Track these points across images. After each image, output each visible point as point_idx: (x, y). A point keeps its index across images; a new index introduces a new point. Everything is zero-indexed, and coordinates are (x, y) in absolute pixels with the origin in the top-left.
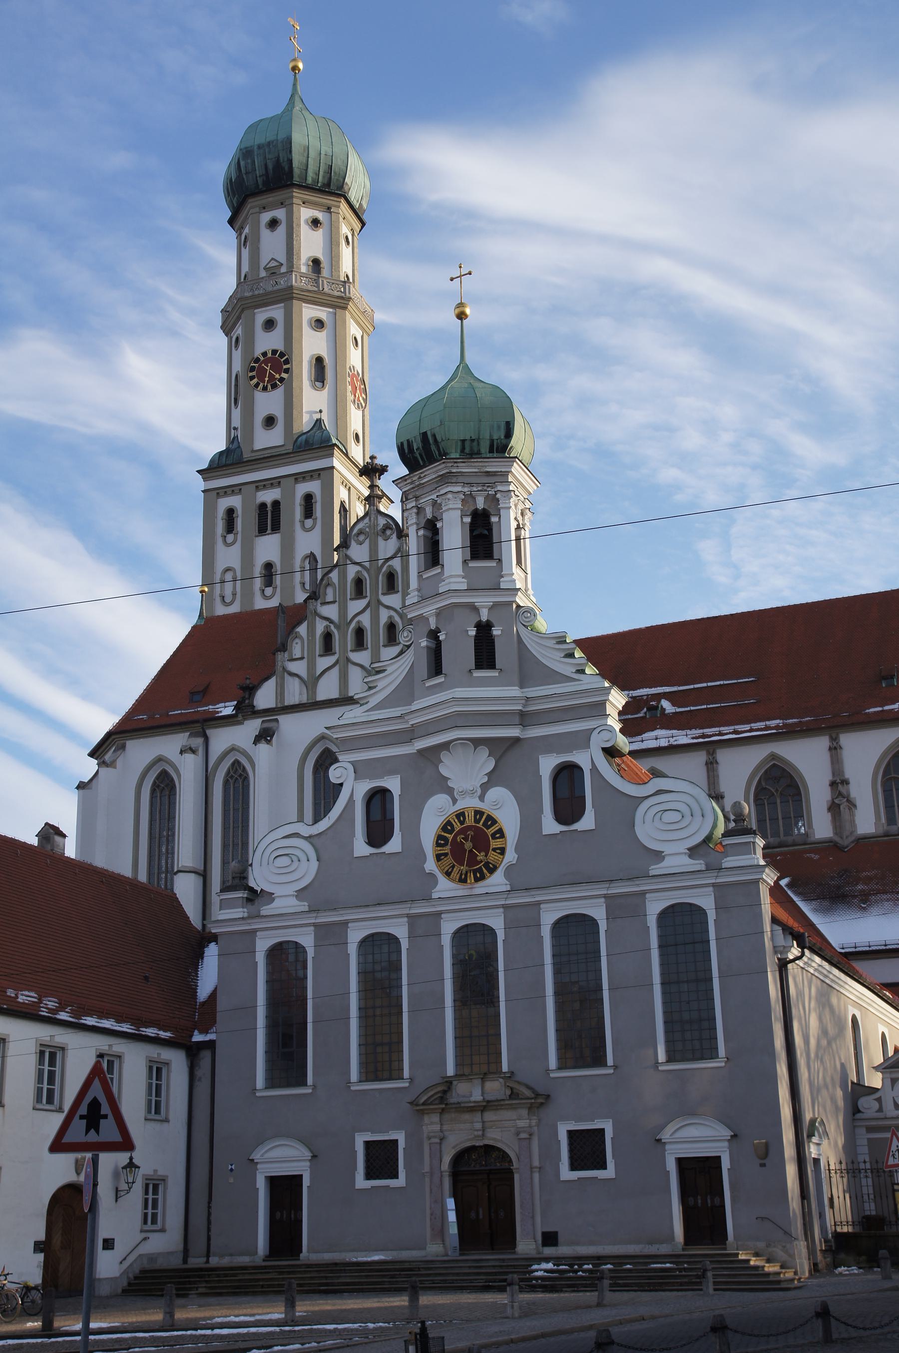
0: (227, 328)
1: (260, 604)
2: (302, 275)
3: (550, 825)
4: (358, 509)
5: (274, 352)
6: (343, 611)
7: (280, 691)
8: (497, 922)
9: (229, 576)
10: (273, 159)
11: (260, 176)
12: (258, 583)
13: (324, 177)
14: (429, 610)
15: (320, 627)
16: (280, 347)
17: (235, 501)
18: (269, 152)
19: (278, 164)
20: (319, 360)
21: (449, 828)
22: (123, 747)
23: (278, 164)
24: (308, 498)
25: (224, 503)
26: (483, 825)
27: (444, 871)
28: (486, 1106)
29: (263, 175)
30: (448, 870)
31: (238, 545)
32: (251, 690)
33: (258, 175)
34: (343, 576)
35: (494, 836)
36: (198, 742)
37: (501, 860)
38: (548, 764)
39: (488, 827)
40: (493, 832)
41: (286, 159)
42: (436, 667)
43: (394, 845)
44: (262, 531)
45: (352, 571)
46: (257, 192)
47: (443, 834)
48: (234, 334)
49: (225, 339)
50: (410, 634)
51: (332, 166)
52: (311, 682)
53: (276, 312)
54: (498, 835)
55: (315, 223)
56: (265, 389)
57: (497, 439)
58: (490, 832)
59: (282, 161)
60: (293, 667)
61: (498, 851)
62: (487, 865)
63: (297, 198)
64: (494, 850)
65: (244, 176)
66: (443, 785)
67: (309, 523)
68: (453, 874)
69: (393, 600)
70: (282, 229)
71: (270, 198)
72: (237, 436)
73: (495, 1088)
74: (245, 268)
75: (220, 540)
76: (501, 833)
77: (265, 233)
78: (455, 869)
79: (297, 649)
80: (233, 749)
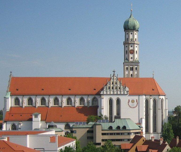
5: (132, 50)
20: (136, 51)
25: (126, 67)
53: (132, 45)
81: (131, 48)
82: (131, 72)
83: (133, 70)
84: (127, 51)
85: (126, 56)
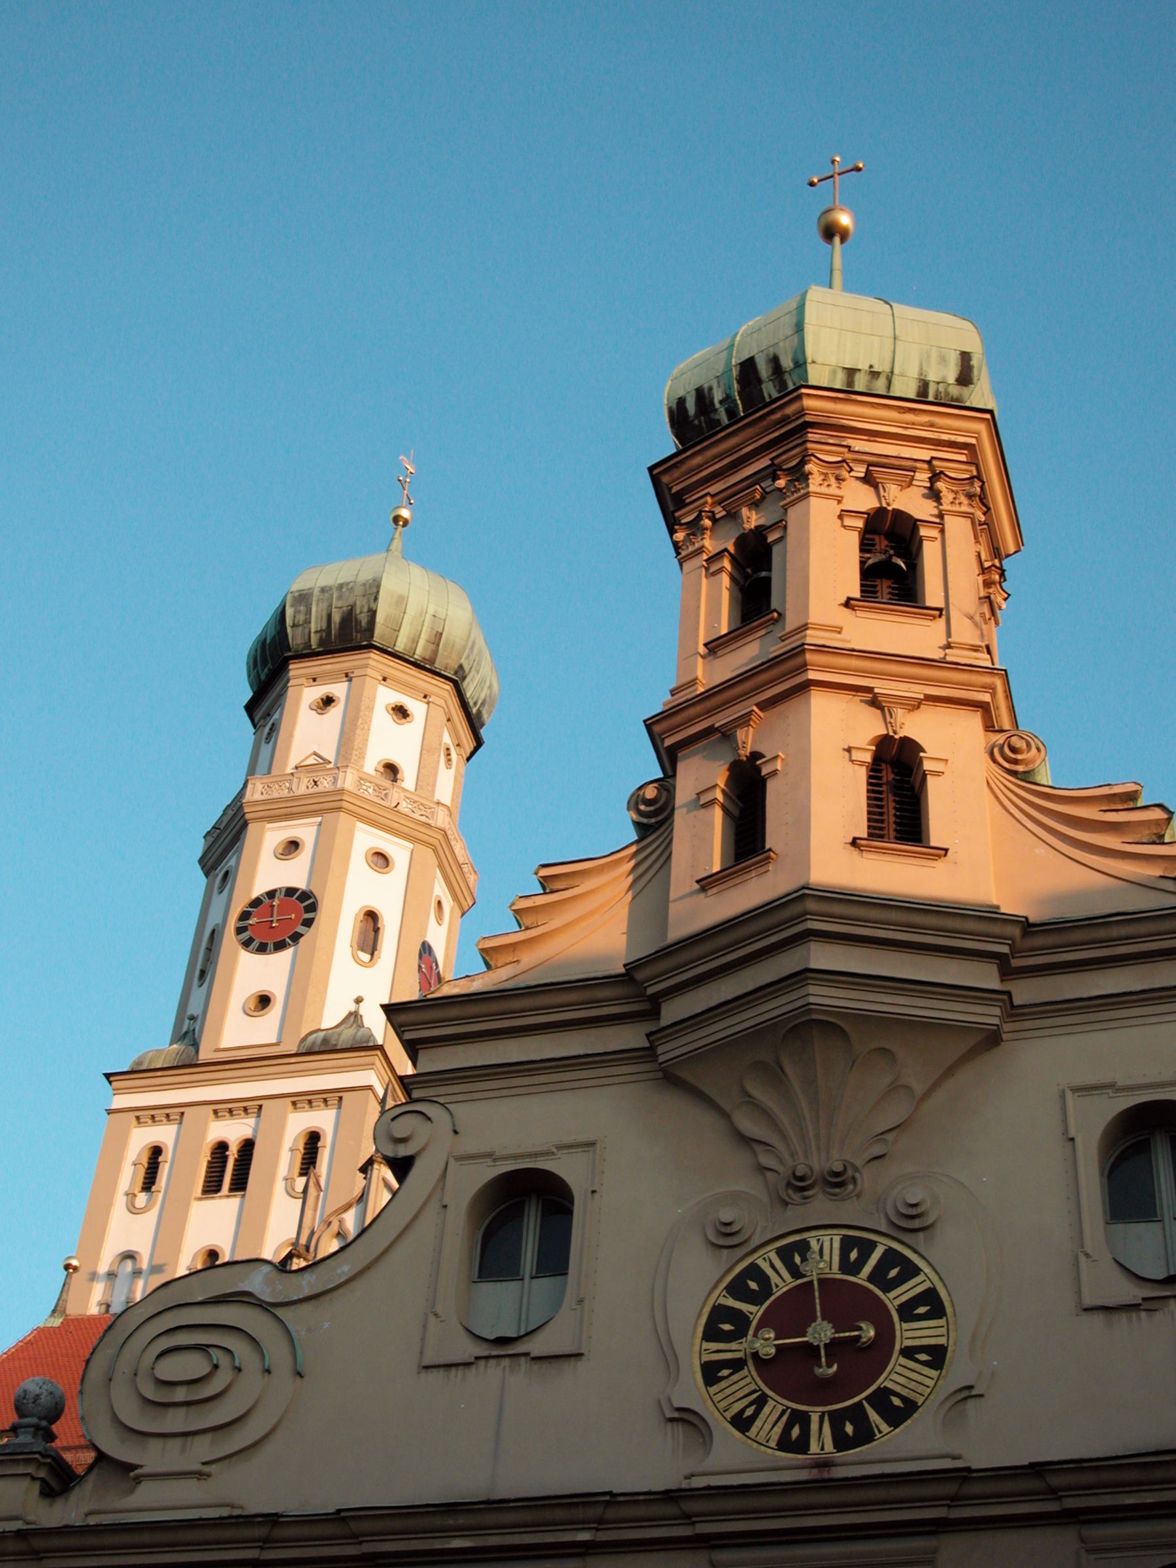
2: (362, 779)
10: (345, 609)
11: (316, 632)
13: (425, 648)
18: (340, 598)
19: (349, 617)
21: (753, 1285)
26: (871, 1278)
27: (729, 1415)
29: (321, 631)
30: (743, 1411)
31: (155, 1210)
33: (313, 630)
35: (907, 1312)
37: (931, 1383)
39: (888, 1286)
40: (904, 1298)
41: (365, 609)
47: (731, 1302)
48: (221, 871)
50: (665, 794)
51: (441, 634)
54: (922, 1310)
55: (401, 712)
56: (262, 949)
57: (938, 383)
58: (894, 1299)
59: (358, 612)
61: (923, 1357)
62: (881, 1399)
63: (374, 669)
64: (908, 1353)
65: (289, 630)
68: (758, 1423)
72: (194, 1030)
75: (120, 1201)
78: (766, 1410)
83: (240, 1184)
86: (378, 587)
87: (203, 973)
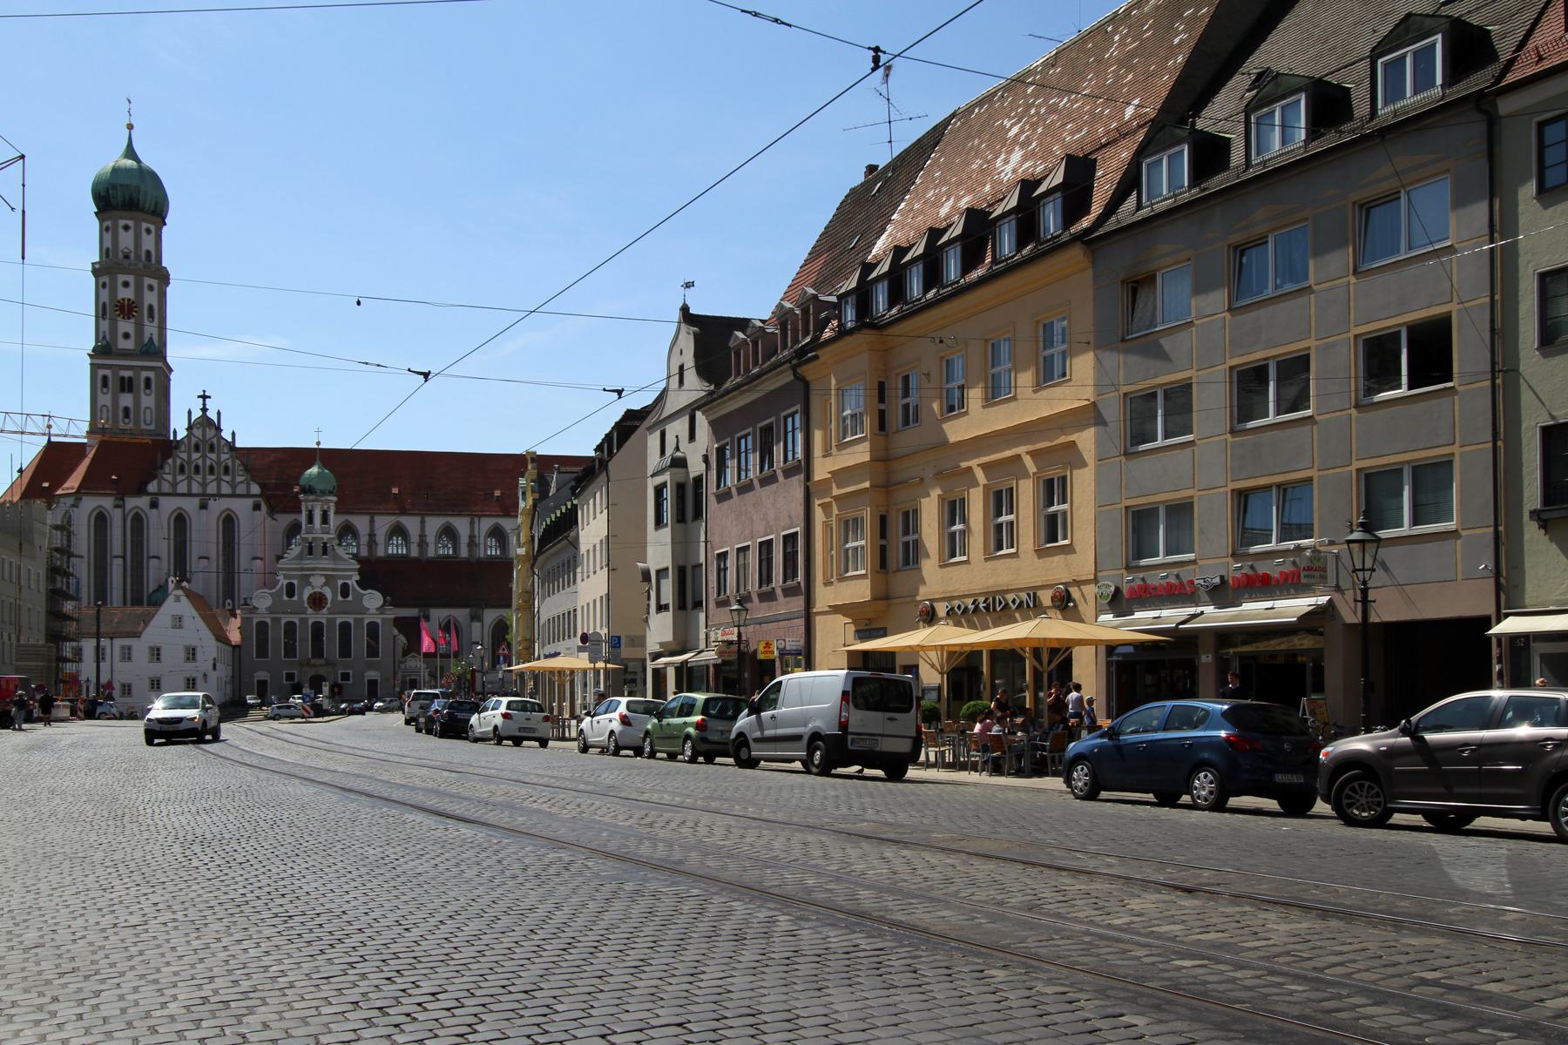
0: (96, 272)
1: (122, 426)
3: (340, 598)
4: (197, 414)
6: (189, 456)
7: (159, 485)
8: (324, 621)
9: (104, 408)
12: (121, 415)
14: (310, 537)
15: (179, 462)
16: (132, 297)
17: (108, 373)
19: (131, 198)
22: (81, 499)
23: (131, 198)
24: (148, 380)
25: (101, 372)
28: (321, 665)
32: (146, 484)
34: (189, 441)
36: (121, 502)
38: (340, 582)
42: (310, 553)
43: (295, 598)
44: (123, 390)
45: (194, 440)
46: (116, 208)
49: (93, 279)
52: (174, 485)
53: (131, 279)
55: (148, 231)
60: (166, 477)
66: (309, 584)
67: (148, 391)
69: (213, 456)
70: (131, 232)
71: (124, 213)
73: (321, 661)
74: (108, 244)
76: (326, 599)
77: (121, 231)
79: (167, 470)
80: (137, 507)
81: (126, 294)
82: (126, 400)
84: (104, 304)
85: (102, 329)
86: (139, 191)
87: (104, 313)
